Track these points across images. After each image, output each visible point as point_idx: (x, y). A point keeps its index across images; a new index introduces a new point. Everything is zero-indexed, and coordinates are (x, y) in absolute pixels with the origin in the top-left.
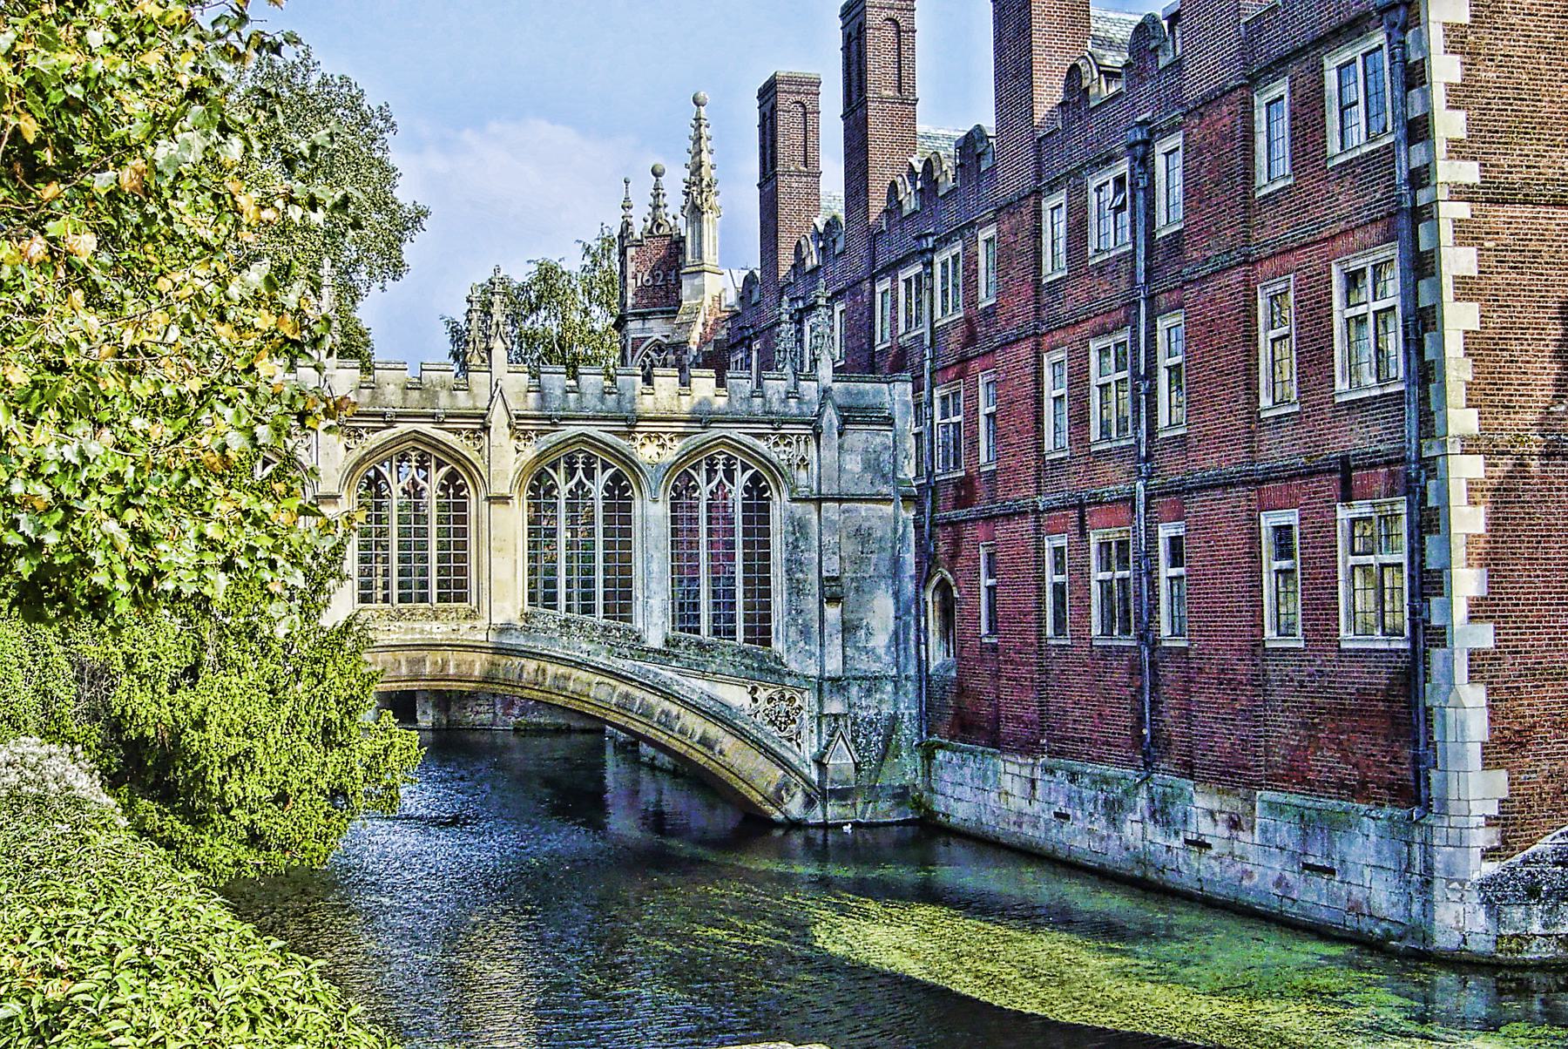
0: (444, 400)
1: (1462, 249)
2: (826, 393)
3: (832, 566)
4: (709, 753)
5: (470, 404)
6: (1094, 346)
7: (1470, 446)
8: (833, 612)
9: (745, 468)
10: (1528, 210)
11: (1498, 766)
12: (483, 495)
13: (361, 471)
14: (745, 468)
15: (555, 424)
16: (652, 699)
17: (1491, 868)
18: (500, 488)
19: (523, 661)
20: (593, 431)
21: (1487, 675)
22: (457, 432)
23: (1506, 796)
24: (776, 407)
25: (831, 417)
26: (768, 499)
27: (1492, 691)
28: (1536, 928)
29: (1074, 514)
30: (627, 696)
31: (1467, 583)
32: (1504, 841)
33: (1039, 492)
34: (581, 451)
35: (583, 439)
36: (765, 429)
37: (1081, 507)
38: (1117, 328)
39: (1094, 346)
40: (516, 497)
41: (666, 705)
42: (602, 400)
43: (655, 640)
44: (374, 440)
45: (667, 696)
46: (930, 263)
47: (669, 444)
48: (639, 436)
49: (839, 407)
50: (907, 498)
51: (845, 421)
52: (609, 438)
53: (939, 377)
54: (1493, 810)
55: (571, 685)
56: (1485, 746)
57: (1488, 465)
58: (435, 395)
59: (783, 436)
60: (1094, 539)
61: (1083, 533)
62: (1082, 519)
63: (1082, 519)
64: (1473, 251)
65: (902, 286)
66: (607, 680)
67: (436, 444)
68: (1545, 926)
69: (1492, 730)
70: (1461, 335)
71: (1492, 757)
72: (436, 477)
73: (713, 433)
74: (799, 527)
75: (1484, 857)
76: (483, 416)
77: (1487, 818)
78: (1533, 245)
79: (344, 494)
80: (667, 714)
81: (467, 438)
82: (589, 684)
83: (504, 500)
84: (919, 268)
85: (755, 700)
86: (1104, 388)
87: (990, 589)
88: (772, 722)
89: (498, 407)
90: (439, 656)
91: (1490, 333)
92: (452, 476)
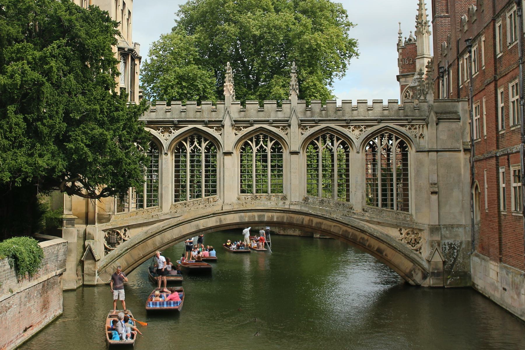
2: (430, 107)
3: (435, 179)
4: (381, 255)
5: (283, 116)
6: (510, 85)
8: (434, 197)
9: (397, 139)
12: (288, 152)
14: (397, 139)
15: (316, 123)
16: (357, 233)
19: (303, 216)
20: (332, 125)
22: (278, 127)
24: (409, 114)
25: (433, 118)
26: (407, 151)
29: (506, 157)
30: (346, 231)
33: (498, 148)
34: (328, 133)
35: (328, 129)
36: (405, 123)
37: (508, 154)
38: (515, 78)
39: (510, 85)
40: (301, 152)
41: (363, 235)
42: (335, 113)
44: (245, 131)
46: (470, 52)
48: (352, 127)
49: (436, 113)
50: (465, 150)
51: (439, 119)
53: (474, 98)
59: (412, 126)
60: (512, 169)
61: (509, 166)
62: (508, 159)
63: (508, 159)
65: (465, 61)
67: (270, 132)
72: (270, 144)
73: (382, 125)
74: (420, 164)
76: (287, 121)
79: (234, 152)
80: (363, 239)
81: (282, 129)
82: (331, 226)
83: (296, 153)
84: (468, 55)
85: (401, 234)
86: (513, 102)
87: (504, 188)
88: (408, 243)
90: (270, 214)
92: (276, 144)
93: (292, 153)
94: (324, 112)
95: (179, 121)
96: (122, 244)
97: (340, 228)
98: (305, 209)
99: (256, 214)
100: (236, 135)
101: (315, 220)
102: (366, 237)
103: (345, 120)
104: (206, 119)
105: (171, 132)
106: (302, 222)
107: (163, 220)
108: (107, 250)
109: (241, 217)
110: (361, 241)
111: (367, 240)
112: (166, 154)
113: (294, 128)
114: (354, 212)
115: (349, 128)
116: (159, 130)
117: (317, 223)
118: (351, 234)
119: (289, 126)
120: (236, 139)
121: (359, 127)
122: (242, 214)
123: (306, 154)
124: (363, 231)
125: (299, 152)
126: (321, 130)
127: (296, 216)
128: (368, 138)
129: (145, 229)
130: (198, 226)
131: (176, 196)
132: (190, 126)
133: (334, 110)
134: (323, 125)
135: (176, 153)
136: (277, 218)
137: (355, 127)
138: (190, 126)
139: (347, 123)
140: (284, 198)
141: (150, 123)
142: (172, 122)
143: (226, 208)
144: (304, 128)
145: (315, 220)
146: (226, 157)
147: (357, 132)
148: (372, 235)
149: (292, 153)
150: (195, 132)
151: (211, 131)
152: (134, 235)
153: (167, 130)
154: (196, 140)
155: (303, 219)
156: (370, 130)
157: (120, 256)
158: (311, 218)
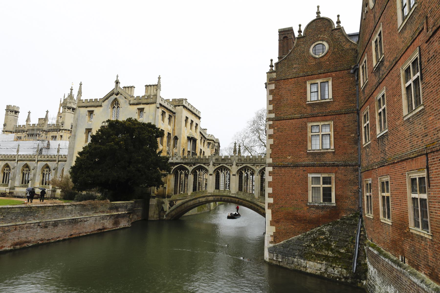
0: (227, 161)
7: (270, 165)
10: (284, 121)
11: (273, 226)
17: (271, 245)
18: (234, 173)
20: (248, 165)
23: (275, 231)
27: (272, 211)
28: (275, 259)
31: (269, 190)
35: (246, 166)
41: (258, 207)
44: (217, 167)
54: (272, 234)
56: (271, 221)
64: (273, 130)
67: (226, 167)
69: (272, 218)
71: (272, 224)
78: (285, 127)
90: (224, 198)
93: (233, 175)
95: (195, 163)
96: (174, 206)
98: (236, 196)
99: (219, 197)
101: (241, 201)
102: (259, 208)
108: (169, 208)
109: (214, 198)
113: (234, 166)
120: (214, 169)
123: (238, 176)
124: (258, 206)
126: (244, 167)
127: (233, 199)
128: (261, 170)
129: (182, 201)
130: (199, 201)
134: (244, 165)
138: (199, 165)
143: (210, 194)
144: (238, 166)
145: (241, 201)
147: (258, 168)
149: (233, 175)
152: (179, 203)
153: (191, 166)
157: (173, 210)
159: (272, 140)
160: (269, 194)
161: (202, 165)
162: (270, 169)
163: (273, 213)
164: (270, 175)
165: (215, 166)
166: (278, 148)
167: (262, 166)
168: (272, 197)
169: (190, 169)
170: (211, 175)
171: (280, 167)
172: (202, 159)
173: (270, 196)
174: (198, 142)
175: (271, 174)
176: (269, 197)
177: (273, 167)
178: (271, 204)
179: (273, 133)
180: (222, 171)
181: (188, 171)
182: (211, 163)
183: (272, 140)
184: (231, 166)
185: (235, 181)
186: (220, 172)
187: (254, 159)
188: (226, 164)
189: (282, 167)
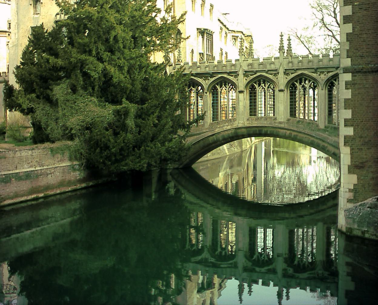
1: (346, 7)
5: (274, 67)
7: (346, 70)
11: (354, 173)
12: (277, 90)
13: (250, 85)
15: (295, 71)
16: (320, 142)
18: (282, 87)
19: (286, 131)
20: (306, 72)
21: (350, 144)
22: (271, 74)
23: (356, 183)
27: (352, 150)
30: (313, 141)
32: (354, 197)
34: (303, 77)
35: (302, 74)
41: (324, 144)
43: (322, 126)
44: (252, 77)
45: (323, 141)
47: (327, 74)
48: (318, 73)
52: (310, 74)
55: (298, 137)
56: (349, 166)
57: (352, 76)
58: (266, 65)
64: (351, 6)
66: (308, 136)
67: (266, 77)
68: (358, 226)
70: (345, 35)
75: (348, 202)
76: (277, 70)
77: (349, 190)
80: (324, 146)
82: (303, 137)
89: (281, 67)
91: (355, 33)
93: (280, 91)
94: (300, 63)
97: (309, 138)
98: (286, 126)
99: (257, 129)
100: (246, 80)
102: (326, 145)
103: (314, 68)
104: (228, 71)
105: (209, 80)
106: (285, 135)
107: (205, 132)
110: (323, 147)
111: (327, 147)
112: (206, 93)
113: (281, 75)
114: (319, 128)
115: (317, 74)
116: (202, 78)
117: (294, 135)
118: (316, 143)
119: (278, 73)
120: (245, 82)
121: (323, 72)
122: (249, 129)
125: (284, 90)
128: (328, 80)
131: (213, 118)
132: (220, 76)
133: (307, 62)
134: (299, 72)
135: (212, 92)
136: (270, 132)
137: (321, 72)
138: (220, 76)
139: (316, 70)
140: (275, 119)
141: (197, 75)
142: (209, 73)
146: (240, 94)
147: (322, 76)
148: (328, 143)
149: (280, 91)
150: (223, 79)
151: (231, 78)
154: (223, 84)
155: (286, 133)
156: (331, 74)
158: (291, 132)
159: (350, 25)
160: (346, 120)
161: (225, 76)
162: (348, 77)
163: (351, 154)
164: (347, 88)
165: (247, 76)
166: (362, 39)
167: (328, 72)
168: (352, 125)
169: (206, 83)
170: (241, 92)
171: (366, 72)
172: (225, 66)
173: (347, 123)
174: (216, 37)
175: (349, 86)
176: (345, 126)
177: (352, 73)
178: (350, 136)
179: (351, 14)
180: (259, 85)
181: (202, 88)
182: (241, 73)
183: (350, 25)
184: (275, 75)
185: (283, 99)
186: (256, 86)
187: (316, 61)
188: (267, 72)
189: (369, 72)
